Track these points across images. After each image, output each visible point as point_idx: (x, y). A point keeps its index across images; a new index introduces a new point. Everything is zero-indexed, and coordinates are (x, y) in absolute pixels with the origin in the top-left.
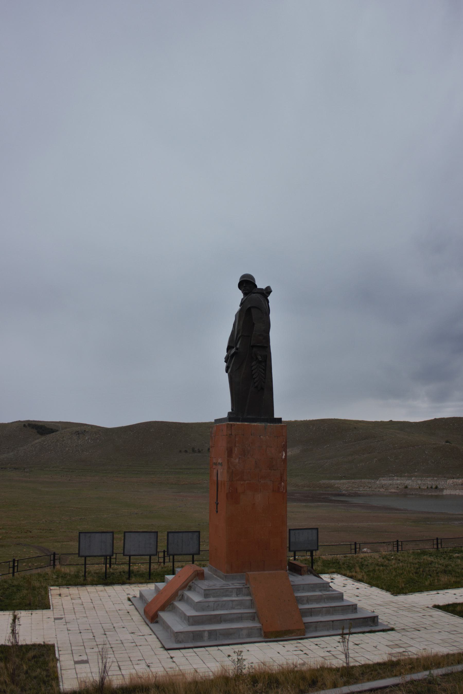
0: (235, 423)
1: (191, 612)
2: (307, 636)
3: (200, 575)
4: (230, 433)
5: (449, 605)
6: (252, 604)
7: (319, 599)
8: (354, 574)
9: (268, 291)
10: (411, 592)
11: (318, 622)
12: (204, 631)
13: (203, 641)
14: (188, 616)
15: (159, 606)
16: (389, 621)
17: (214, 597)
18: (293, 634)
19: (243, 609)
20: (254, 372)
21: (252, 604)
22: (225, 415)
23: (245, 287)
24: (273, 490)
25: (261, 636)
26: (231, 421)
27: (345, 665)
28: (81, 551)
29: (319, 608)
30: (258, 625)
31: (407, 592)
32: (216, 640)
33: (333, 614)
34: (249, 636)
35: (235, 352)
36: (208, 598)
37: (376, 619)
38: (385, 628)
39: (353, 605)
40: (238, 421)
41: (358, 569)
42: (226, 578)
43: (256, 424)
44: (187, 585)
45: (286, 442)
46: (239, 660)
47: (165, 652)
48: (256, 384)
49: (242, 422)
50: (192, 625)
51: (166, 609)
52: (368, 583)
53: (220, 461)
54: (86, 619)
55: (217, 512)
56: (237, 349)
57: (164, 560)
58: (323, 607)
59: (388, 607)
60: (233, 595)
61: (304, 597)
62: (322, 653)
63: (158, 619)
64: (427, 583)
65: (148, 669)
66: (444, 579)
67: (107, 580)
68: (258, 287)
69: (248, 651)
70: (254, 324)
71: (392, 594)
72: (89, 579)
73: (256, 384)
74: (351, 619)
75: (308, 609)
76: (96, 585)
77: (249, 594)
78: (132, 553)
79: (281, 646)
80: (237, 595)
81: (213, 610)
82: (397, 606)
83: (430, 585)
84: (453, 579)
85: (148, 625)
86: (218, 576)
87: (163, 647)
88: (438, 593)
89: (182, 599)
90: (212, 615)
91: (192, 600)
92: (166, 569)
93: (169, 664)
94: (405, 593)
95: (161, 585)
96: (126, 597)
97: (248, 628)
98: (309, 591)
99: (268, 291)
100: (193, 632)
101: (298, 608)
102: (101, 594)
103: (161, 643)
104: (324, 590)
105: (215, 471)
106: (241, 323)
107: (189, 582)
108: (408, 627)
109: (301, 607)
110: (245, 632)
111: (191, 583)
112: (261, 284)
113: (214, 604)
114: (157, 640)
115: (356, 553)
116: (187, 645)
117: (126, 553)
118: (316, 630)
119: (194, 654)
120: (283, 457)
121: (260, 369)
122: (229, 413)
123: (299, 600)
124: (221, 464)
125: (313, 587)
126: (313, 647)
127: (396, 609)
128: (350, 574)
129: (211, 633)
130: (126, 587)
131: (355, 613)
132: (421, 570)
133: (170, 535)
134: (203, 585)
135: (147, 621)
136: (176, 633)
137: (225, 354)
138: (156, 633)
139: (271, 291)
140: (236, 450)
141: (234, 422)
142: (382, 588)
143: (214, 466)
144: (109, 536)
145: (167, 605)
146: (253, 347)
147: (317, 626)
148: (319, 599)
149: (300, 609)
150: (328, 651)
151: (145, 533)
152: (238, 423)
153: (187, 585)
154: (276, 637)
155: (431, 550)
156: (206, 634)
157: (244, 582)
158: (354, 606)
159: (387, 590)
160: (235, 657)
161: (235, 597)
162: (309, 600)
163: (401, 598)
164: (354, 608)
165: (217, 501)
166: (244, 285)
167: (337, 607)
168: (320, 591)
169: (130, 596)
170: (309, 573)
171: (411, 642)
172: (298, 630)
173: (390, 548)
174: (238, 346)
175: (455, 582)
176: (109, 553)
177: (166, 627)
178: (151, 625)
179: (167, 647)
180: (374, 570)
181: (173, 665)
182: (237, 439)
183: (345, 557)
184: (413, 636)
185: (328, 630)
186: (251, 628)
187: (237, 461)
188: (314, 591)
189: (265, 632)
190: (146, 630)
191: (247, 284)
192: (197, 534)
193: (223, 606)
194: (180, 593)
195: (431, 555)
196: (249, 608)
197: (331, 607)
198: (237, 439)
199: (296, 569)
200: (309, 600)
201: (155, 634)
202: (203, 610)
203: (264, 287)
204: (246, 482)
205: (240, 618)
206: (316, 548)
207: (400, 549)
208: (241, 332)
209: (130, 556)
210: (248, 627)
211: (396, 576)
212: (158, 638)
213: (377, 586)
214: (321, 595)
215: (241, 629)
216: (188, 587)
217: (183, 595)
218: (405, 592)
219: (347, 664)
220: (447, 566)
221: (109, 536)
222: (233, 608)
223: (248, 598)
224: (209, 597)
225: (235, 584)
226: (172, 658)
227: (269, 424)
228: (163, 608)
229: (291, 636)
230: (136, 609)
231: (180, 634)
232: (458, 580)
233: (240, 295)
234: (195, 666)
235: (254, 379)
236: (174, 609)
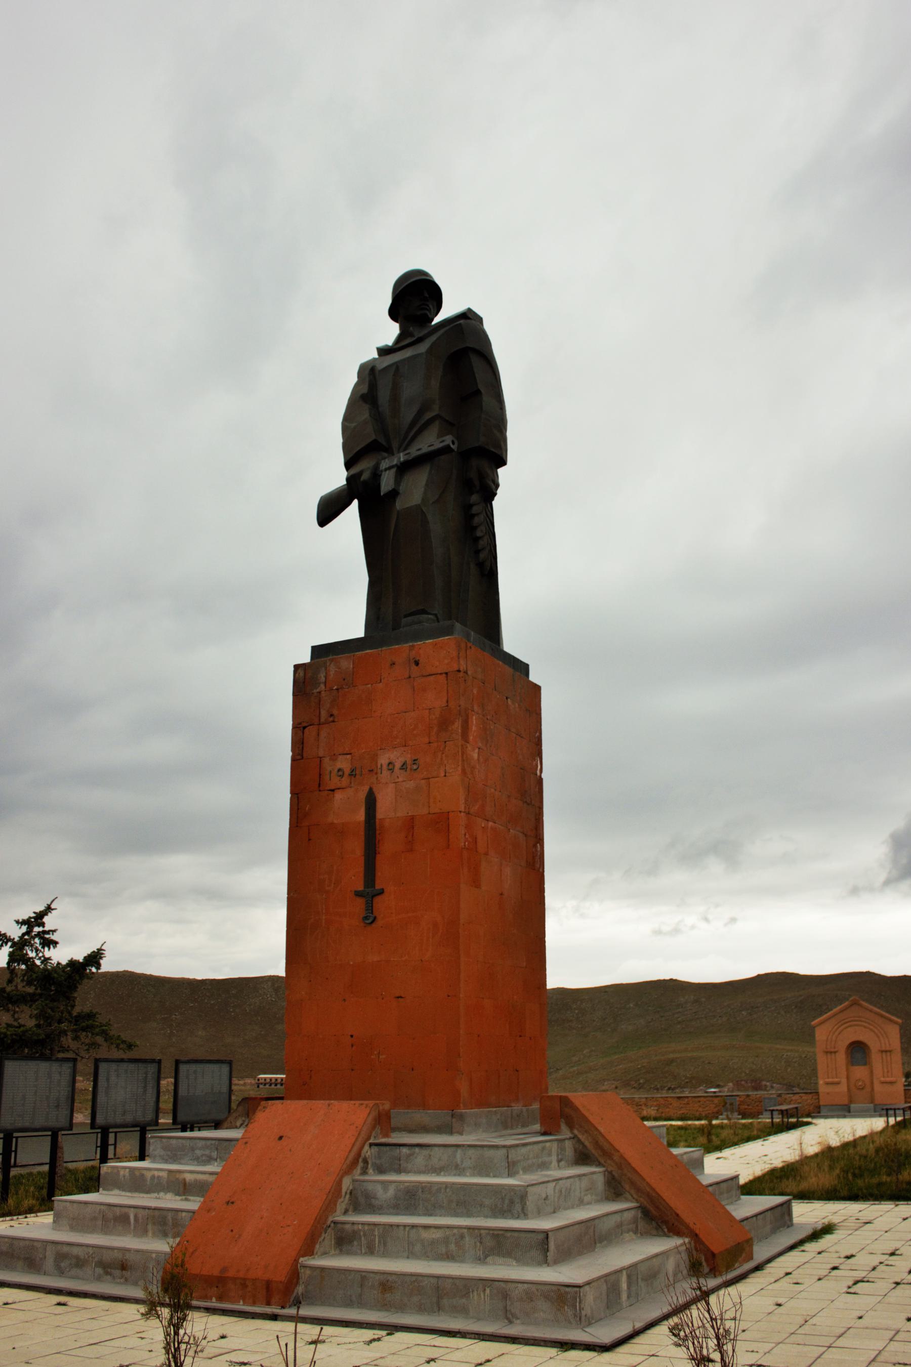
6: (615, 1189)
17: (526, 1170)
44: (359, 1154)
50: (556, 1262)
77: (583, 1158)
89: (361, 1201)
110: (670, 1265)
111: (366, 1147)
153: (359, 1154)
194: (347, 1183)
216: (361, 1164)
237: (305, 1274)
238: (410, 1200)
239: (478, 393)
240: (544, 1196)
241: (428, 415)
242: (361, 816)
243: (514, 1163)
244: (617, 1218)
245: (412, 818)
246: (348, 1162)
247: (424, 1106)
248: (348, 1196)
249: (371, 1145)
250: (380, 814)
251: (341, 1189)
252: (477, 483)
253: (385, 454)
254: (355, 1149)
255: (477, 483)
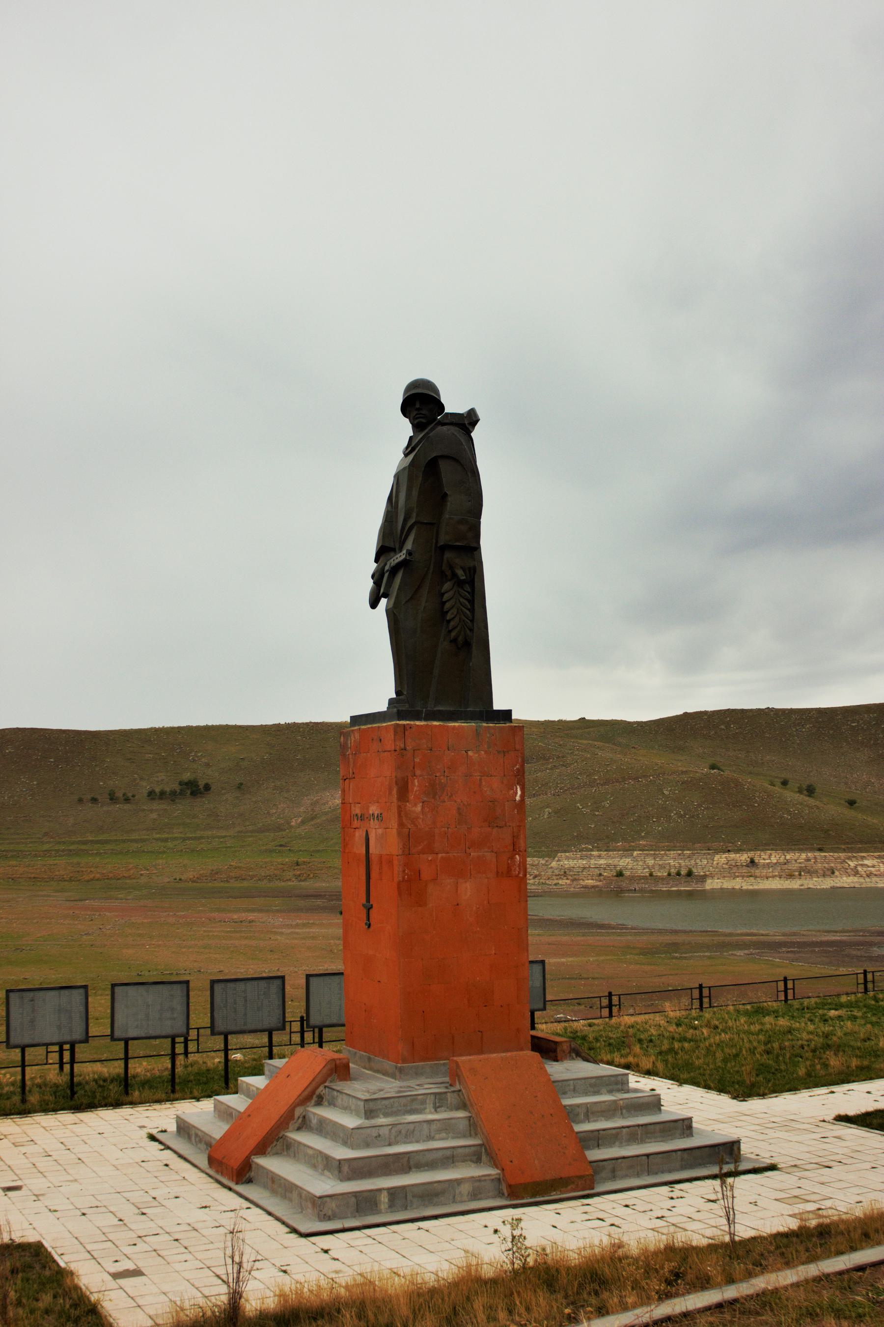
0: (412, 723)
1: (341, 1153)
2: (598, 1189)
3: (340, 1070)
4: (402, 746)
5: (868, 1114)
6: (473, 1127)
7: (611, 1110)
8: (631, 1059)
9: (468, 421)
10: (774, 1092)
11: (617, 1159)
12: (380, 1190)
13: (379, 1212)
14: (340, 1161)
15: (252, 1143)
16: (757, 1151)
17: (386, 1115)
18: (569, 1187)
19: (453, 1138)
20: (447, 605)
21: (473, 1127)
22: (383, 707)
23: (418, 409)
24: (498, 873)
25: (500, 1194)
26: (403, 719)
27: (727, 1239)
28: (12, 1034)
29: (614, 1128)
30: (493, 1172)
31: (766, 1091)
32: (406, 1209)
33: (643, 1141)
34: (475, 1195)
35: (405, 560)
36: (373, 1118)
37: (735, 1148)
38: (757, 1165)
39: (683, 1120)
40: (419, 719)
41: (637, 1049)
42: (399, 1073)
43: (456, 724)
44: (313, 1092)
45: (523, 766)
46: (514, 1237)
47: (303, 1240)
48: (453, 634)
49: (426, 719)
50: (349, 1179)
51: (269, 1149)
52: (672, 1078)
53: (374, 809)
54: (75, 1187)
55: (369, 926)
56: (409, 553)
57: (186, 1047)
58: (623, 1127)
59: (738, 1124)
60: (428, 1110)
61: (578, 1106)
62: (645, 1222)
63: (252, 1174)
64: (802, 1072)
65: (287, 1276)
66: (835, 1062)
67: (76, 1097)
68: (447, 410)
69: (486, 1226)
70: (445, 495)
71: (734, 1098)
72: (34, 1099)
73: (453, 634)
74: (685, 1150)
75: (592, 1131)
76: (55, 1110)
77: (463, 1106)
78: (132, 1033)
79: (552, 1214)
80: (436, 1109)
81: (390, 1145)
82: (757, 1121)
83: (809, 1075)
84: (855, 1062)
85: (230, 1189)
86: (378, 1071)
87: (294, 1231)
88: (833, 1092)
89: (304, 1125)
90: (390, 1155)
91: (335, 1124)
92: (195, 1069)
93: (326, 1265)
94: (763, 1095)
95: (236, 1102)
96: (144, 1133)
97: (472, 1179)
98: (586, 1093)
99: (469, 421)
100: (355, 1194)
101: (573, 1130)
102: (78, 1129)
103: (284, 1223)
104: (619, 1091)
105: (359, 835)
106: (415, 493)
107: (317, 1087)
108: (802, 1162)
109: (578, 1128)
110: (465, 1188)
111: (321, 1088)
112: (453, 404)
113: (390, 1130)
114: (270, 1218)
115: (611, 1015)
116: (348, 1224)
117: (117, 1034)
118: (614, 1177)
119: (370, 1241)
120: (518, 798)
121: (462, 600)
122: (391, 701)
123: (572, 1114)
124: (380, 817)
125: (595, 1085)
126: (622, 1211)
127: (757, 1127)
128: (623, 1061)
129: (393, 1192)
130: (125, 1111)
131: (688, 1136)
132: (776, 1045)
133: (218, 988)
134: (359, 1089)
135: (225, 1181)
136: (320, 1197)
137: (372, 566)
138: (261, 1203)
139: (478, 420)
140: (415, 784)
141: (406, 719)
142: (707, 1087)
143: (356, 823)
144: (77, 996)
145: (273, 1141)
146: (443, 548)
147: (615, 1168)
148: (611, 1110)
149: (577, 1133)
150: (658, 1218)
151: (161, 986)
152: (418, 723)
153: (313, 1092)
154: (534, 1195)
155: (774, 1004)
156: (384, 1198)
157: (447, 1079)
158: (686, 1122)
159: (721, 1090)
160: (506, 1231)
161: (431, 1113)
162: (590, 1112)
163: (755, 1105)
164: (685, 1126)
165: (368, 900)
166: (418, 406)
167: (650, 1124)
168: (610, 1092)
169: (154, 1132)
170: (574, 1055)
171: (826, 1191)
172: (580, 1177)
173: (685, 1001)
174: (409, 545)
175: (861, 1068)
176: (78, 1035)
177: (283, 1189)
178: (239, 1188)
179: (303, 1229)
180: (671, 1050)
181: (337, 1265)
182: (417, 760)
183: (590, 1025)
184: (823, 1179)
185: (638, 1175)
186: (479, 1179)
187: (419, 808)
188: (597, 1093)
189: (510, 1186)
190: (230, 1200)
191: (421, 402)
192: (278, 982)
193: (409, 1134)
194: (298, 1111)
195: (776, 1014)
196: (464, 1136)
197: (638, 1126)
198: (417, 760)
199: (547, 1049)
200: (590, 1112)
201: (258, 1206)
202: (367, 1145)
203: (462, 409)
204: (440, 855)
205: (449, 1159)
206: (541, 1006)
207: (706, 1005)
208: (414, 515)
209: (126, 1041)
210: (473, 1177)
211: (725, 1060)
212: (270, 1214)
213: (695, 1083)
214: (615, 1101)
215: (459, 1182)
216: (315, 1098)
217: (304, 1117)
218: (761, 1092)
219: (732, 1234)
220: (826, 1036)
221: (77, 996)
222: (431, 1138)
223: (461, 1114)
224: (378, 1116)
225: (425, 1086)
226: (326, 1251)
227: (485, 725)
228: (262, 1149)
229: (562, 1193)
230: (180, 1156)
231: (328, 1199)
232: (866, 1063)
233: (405, 429)
234: (388, 1264)
235: (449, 621)
236: (289, 1149)
237: (254, 1166)
238: (323, 1128)
239: (446, 495)
240: (375, 1135)
241: (409, 524)
242: (364, 851)
243: (371, 1111)
244: (448, 1153)
245: (381, 856)
246: (301, 1098)
247: (388, 1059)
248: (300, 1120)
249: (325, 1087)
250: (371, 852)
251: (293, 1115)
252: (449, 573)
253: (392, 554)
254: (309, 1089)
255: (449, 573)
